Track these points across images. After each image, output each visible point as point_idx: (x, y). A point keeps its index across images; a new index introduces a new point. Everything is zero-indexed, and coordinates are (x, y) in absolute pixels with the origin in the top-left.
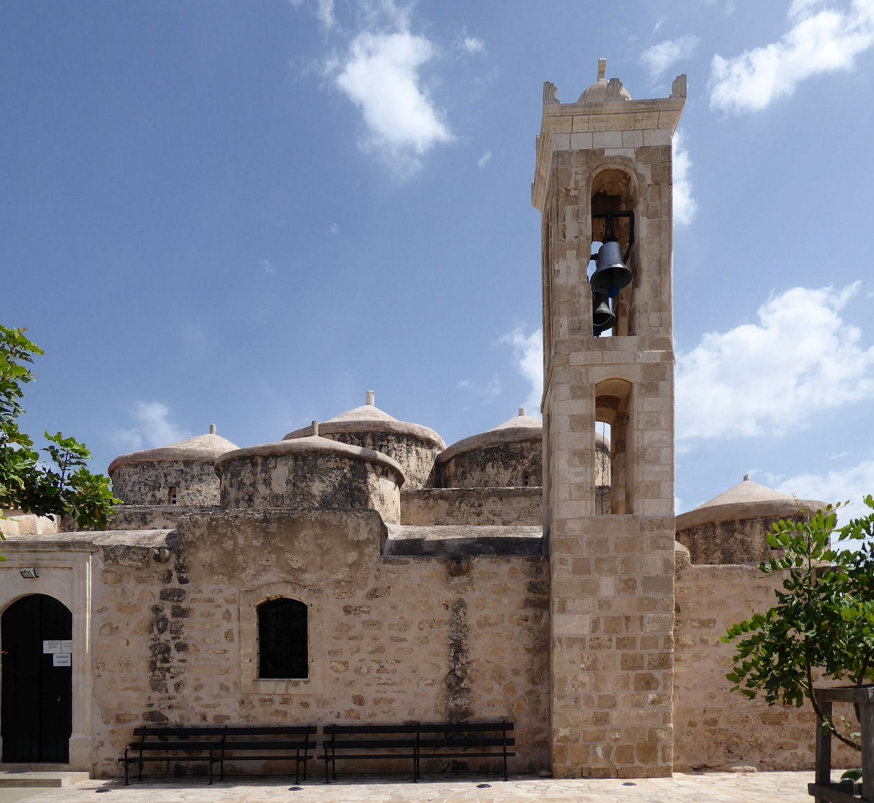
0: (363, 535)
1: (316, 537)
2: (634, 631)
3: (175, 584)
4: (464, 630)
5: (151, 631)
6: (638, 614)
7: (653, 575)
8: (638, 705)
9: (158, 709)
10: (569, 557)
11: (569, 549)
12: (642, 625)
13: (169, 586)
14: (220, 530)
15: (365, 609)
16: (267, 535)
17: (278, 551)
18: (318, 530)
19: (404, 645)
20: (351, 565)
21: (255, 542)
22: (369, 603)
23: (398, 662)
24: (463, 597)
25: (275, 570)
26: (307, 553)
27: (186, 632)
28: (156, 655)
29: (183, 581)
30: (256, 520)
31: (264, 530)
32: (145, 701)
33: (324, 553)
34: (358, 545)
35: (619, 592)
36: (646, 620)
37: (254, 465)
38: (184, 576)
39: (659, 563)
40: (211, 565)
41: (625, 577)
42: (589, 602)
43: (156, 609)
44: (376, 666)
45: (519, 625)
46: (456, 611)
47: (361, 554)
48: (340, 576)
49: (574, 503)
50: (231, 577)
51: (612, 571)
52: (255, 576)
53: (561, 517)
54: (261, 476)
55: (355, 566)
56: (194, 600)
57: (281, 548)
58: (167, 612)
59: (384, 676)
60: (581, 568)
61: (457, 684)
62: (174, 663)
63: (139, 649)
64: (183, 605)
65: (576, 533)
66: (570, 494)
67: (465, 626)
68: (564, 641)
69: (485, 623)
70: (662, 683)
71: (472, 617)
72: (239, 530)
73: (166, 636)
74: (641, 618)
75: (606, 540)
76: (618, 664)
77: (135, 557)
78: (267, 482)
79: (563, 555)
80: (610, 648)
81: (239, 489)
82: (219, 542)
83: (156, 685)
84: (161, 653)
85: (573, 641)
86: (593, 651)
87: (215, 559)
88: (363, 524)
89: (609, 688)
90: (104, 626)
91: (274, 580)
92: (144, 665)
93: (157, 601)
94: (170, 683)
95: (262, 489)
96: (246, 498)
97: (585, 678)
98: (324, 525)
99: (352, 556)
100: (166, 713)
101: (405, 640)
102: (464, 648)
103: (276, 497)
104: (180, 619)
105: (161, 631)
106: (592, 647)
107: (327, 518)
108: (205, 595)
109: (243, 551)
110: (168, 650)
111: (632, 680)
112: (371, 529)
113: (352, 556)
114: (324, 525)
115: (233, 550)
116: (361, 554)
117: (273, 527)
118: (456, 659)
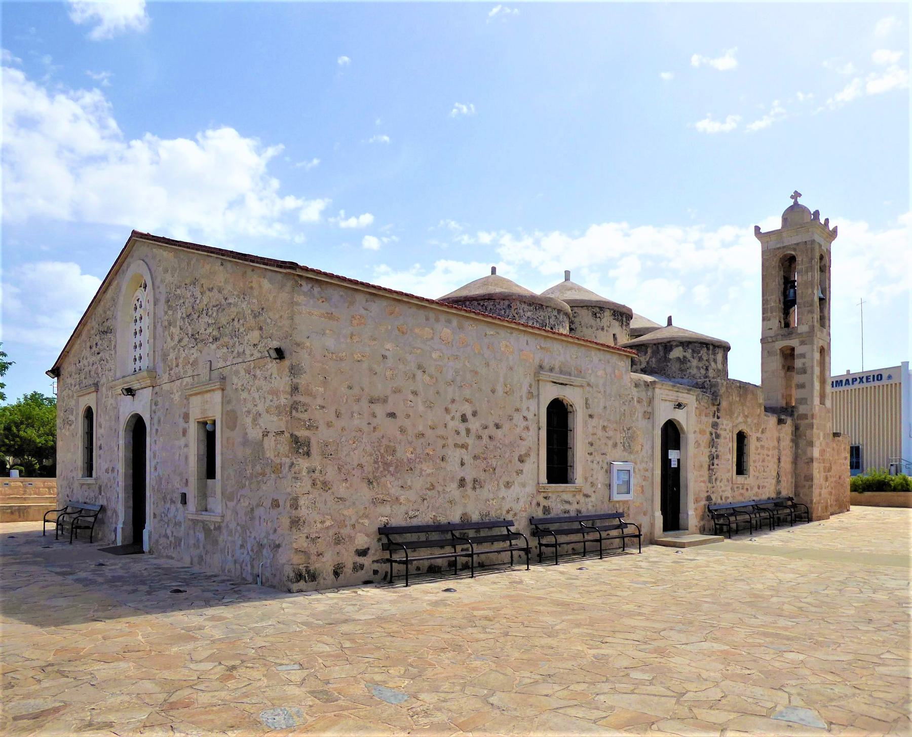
17: (743, 405)
27: (720, 448)
29: (718, 418)
32: (705, 489)
37: (708, 349)
43: (711, 434)
50: (731, 417)
54: (712, 357)
62: (715, 466)
63: (705, 460)
73: (714, 450)
83: (710, 481)
94: (714, 477)
95: (713, 364)
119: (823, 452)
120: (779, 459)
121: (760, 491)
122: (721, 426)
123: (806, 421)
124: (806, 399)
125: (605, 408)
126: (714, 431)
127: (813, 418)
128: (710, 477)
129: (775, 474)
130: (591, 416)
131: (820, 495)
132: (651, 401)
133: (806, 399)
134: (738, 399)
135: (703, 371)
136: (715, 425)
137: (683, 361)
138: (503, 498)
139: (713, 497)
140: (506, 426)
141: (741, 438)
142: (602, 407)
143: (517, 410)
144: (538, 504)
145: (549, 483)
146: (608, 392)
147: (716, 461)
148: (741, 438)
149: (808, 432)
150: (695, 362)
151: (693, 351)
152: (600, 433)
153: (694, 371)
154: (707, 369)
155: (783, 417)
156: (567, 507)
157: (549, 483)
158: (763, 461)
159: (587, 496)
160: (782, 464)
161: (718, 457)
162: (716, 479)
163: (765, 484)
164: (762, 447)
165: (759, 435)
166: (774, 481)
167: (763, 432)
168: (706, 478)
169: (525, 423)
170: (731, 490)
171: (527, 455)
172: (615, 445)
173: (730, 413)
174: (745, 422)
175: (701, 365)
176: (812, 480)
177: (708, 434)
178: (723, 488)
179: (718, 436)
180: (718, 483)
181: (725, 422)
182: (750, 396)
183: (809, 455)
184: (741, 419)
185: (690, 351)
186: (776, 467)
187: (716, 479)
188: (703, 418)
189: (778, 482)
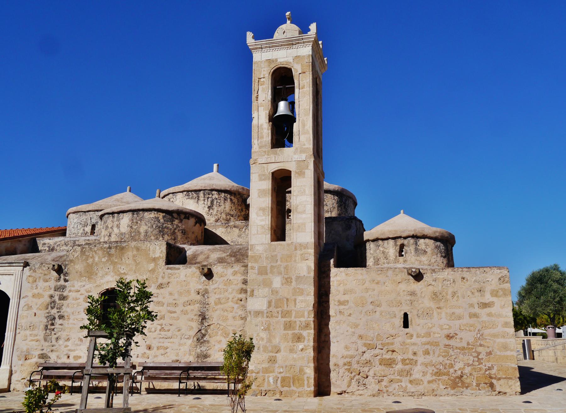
0: (157, 255)
1: (134, 256)
2: (291, 306)
3: (62, 282)
4: (207, 306)
5: (47, 308)
6: (293, 298)
7: (302, 275)
8: (292, 351)
9: (46, 352)
10: (256, 265)
11: (256, 261)
12: (295, 304)
13: (59, 283)
14: (87, 254)
15: (156, 295)
16: (110, 255)
17: (114, 264)
18: (135, 252)
20: (150, 271)
21: (103, 260)
22: (158, 291)
23: (171, 325)
24: (207, 287)
25: (112, 274)
26: (129, 265)
28: (48, 322)
29: (66, 281)
30: (105, 248)
31: (108, 253)
33: (137, 264)
34: (154, 260)
35: (282, 284)
36: (297, 301)
38: (67, 278)
39: (305, 269)
40: (80, 272)
41: (286, 276)
42: (266, 291)
43: (51, 296)
44: (159, 327)
45: (237, 303)
46: (203, 295)
47: (156, 265)
49: (260, 236)
50: (90, 278)
51: (280, 273)
52: (103, 276)
53: (252, 244)
55: (153, 271)
56: (70, 291)
57: (116, 262)
58: (56, 298)
60: (262, 271)
61: (202, 338)
63: (41, 320)
64: (65, 294)
65: (261, 252)
66: (257, 231)
67: (208, 304)
68: (252, 313)
69: (219, 302)
70: (307, 338)
71: (212, 299)
72: (96, 253)
73: (54, 311)
74: (295, 300)
75: (276, 255)
76: (282, 327)
78: (118, 226)
79: (253, 264)
80: (277, 317)
84: (52, 320)
85: (258, 313)
86: (268, 319)
87: (83, 269)
88: (158, 248)
89: (276, 341)
92: (42, 327)
93: (52, 292)
97: (264, 335)
98: (138, 249)
99: (151, 266)
100: (50, 354)
101: (175, 312)
102: (207, 317)
104: (62, 301)
105: (52, 308)
106: (267, 317)
107: (139, 245)
108: (77, 287)
109: (97, 264)
110: (54, 318)
111: (290, 336)
112: (162, 251)
113: (151, 266)
114: (138, 249)
115: (92, 264)
116: (156, 265)
117: (113, 251)
118: (202, 323)
122: (68, 289)
147: (58, 321)
163: (166, 345)
168: (41, 337)
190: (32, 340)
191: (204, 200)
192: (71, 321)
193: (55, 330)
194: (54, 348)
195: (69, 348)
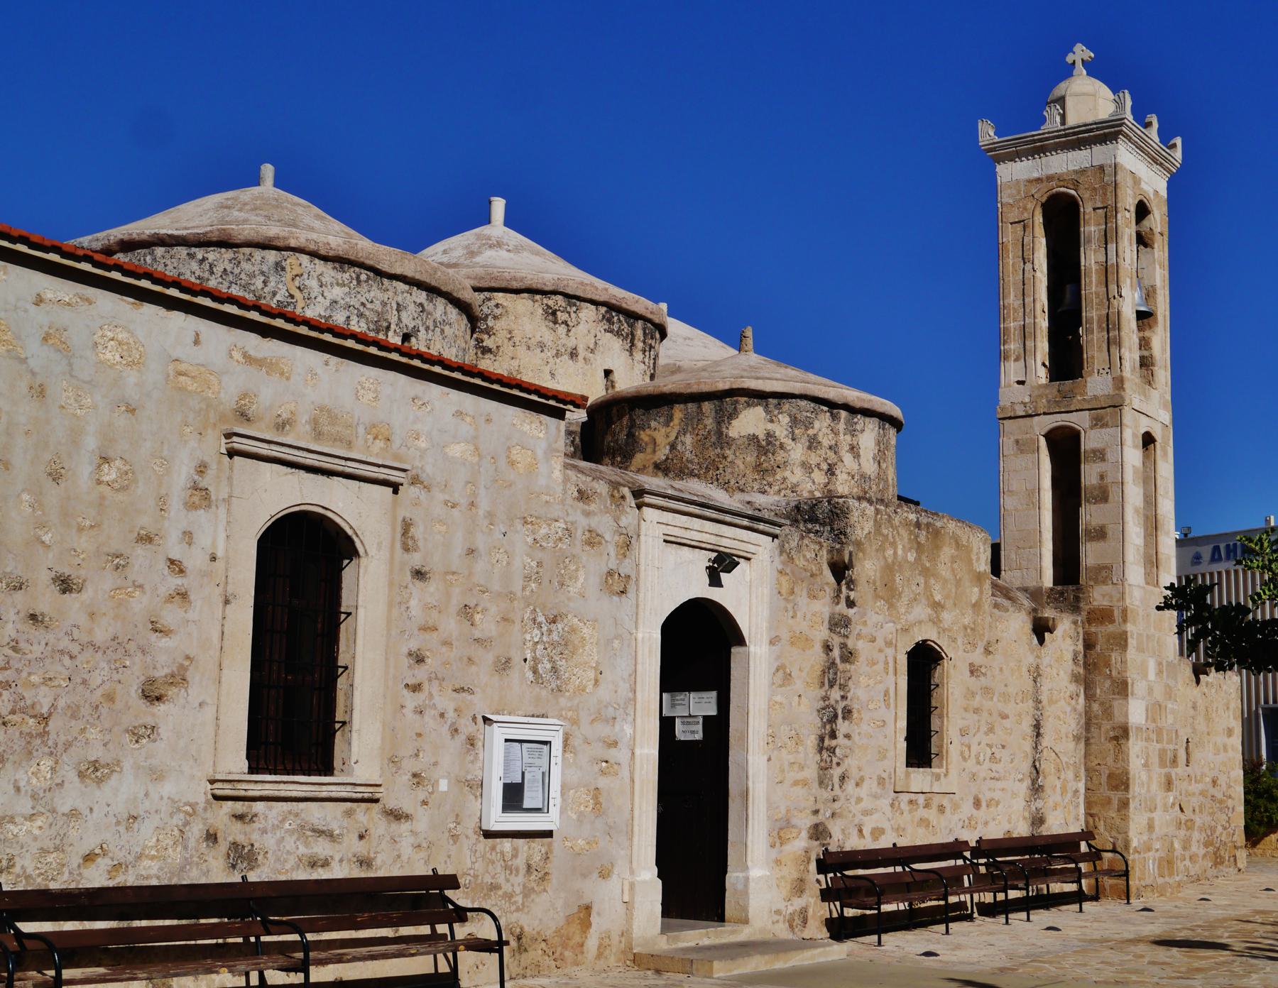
17: (926, 572)
19: (1007, 723)
28: (824, 726)
29: (851, 604)
32: (810, 805)
40: (874, 583)
43: (828, 648)
48: (966, 621)
50: (891, 606)
54: (845, 440)
55: (976, 606)
58: (836, 653)
59: (994, 767)
62: (841, 740)
73: (835, 694)
77: (808, 555)
81: (810, 448)
82: (882, 549)
90: (777, 670)
91: (923, 617)
95: (847, 458)
96: (825, 467)
102: (1042, 731)
103: (863, 476)
115: (893, 563)
116: (981, 592)
119: (1155, 710)
120: (1037, 726)
121: (982, 814)
122: (856, 628)
123: (1111, 628)
124: (1109, 568)
125: (471, 552)
126: (836, 641)
127: (1125, 621)
128: (824, 769)
129: (1026, 767)
130: (419, 574)
131: (1151, 827)
132: (627, 544)
133: (1109, 568)
134: (911, 557)
135: (820, 477)
136: (839, 624)
137: (764, 446)
138: (74, 814)
139: (835, 829)
140: (98, 587)
141: (923, 661)
142: (458, 549)
143: (146, 539)
144: (212, 837)
145: (252, 771)
146: (484, 505)
147: (842, 726)
148: (923, 661)
149: (1115, 657)
150: (797, 452)
151: (795, 421)
152: (451, 625)
153: (795, 475)
154: (831, 471)
155: (1048, 613)
156: (322, 848)
157: (252, 771)
158: (991, 730)
159: (396, 816)
160: (1046, 741)
161: (847, 713)
162: (843, 778)
163: (997, 795)
164: (987, 691)
165: (977, 657)
166: (1024, 788)
167: (987, 652)
168: (811, 773)
169: (176, 582)
170: (887, 811)
171: (179, 678)
172: (504, 665)
173: (889, 592)
174: (936, 621)
175: (814, 459)
176: (1127, 788)
177: (818, 648)
178: (867, 804)
179: (848, 656)
180: (850, 786)
181: (873, 618)
182: (947, 552)
183: (1118, 718)
184: (921, 611)
185: (785, 419)
186: (1028, 745)
187: (843, 778)
188: (802, 599)
189: (1036, 789)
190: (796, 783)
191: (644, 351)
192: (864, 727)
193: (837, 751)
194: (836, 805)
195: (863, 805)
